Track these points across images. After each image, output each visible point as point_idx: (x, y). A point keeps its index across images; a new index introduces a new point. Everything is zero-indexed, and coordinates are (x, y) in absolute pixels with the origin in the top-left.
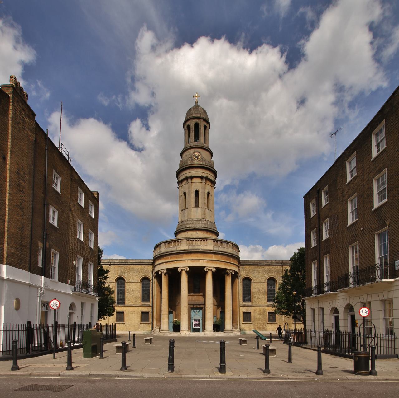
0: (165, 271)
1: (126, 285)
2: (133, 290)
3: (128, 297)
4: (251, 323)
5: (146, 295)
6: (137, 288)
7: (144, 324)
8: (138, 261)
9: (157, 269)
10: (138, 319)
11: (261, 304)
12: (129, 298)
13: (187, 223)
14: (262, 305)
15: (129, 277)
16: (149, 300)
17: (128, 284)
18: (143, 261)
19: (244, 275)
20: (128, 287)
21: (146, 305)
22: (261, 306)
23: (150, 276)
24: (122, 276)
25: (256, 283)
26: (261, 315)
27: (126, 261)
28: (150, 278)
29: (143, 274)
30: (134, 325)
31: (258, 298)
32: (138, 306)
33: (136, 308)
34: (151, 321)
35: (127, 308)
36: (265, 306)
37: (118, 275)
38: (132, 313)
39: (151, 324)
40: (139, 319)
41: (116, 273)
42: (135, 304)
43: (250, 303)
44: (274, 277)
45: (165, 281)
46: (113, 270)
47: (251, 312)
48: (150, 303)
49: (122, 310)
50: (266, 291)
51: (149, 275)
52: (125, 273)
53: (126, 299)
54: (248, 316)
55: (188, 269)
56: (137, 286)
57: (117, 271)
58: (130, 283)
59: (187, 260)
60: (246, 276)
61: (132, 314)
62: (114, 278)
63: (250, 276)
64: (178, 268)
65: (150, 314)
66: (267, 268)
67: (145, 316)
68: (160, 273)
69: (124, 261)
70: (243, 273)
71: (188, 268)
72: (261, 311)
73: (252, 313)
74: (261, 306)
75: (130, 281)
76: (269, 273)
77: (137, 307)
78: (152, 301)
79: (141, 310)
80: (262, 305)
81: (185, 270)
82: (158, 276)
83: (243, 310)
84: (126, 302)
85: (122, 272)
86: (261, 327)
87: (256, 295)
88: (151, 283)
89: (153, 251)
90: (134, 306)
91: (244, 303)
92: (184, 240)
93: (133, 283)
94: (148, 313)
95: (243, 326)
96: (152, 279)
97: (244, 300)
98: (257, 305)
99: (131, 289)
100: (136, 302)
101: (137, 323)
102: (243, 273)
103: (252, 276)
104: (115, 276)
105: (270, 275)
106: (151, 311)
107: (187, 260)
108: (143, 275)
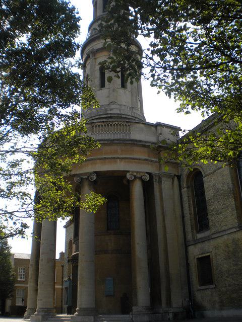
4: (213, 286)
11: (226, 228)
14: (228, 230)
22: (227, 232)
25: (210, 174)
26: (231, 260)
31: (219, 212)
36: (234, 230)
47: (209, 256)
55: (94, 177)
72: (228, 247)
73: (214, 261)
74: (227, 232)
80: (228, 230)
86: (235, 295)
87: (213, 207)
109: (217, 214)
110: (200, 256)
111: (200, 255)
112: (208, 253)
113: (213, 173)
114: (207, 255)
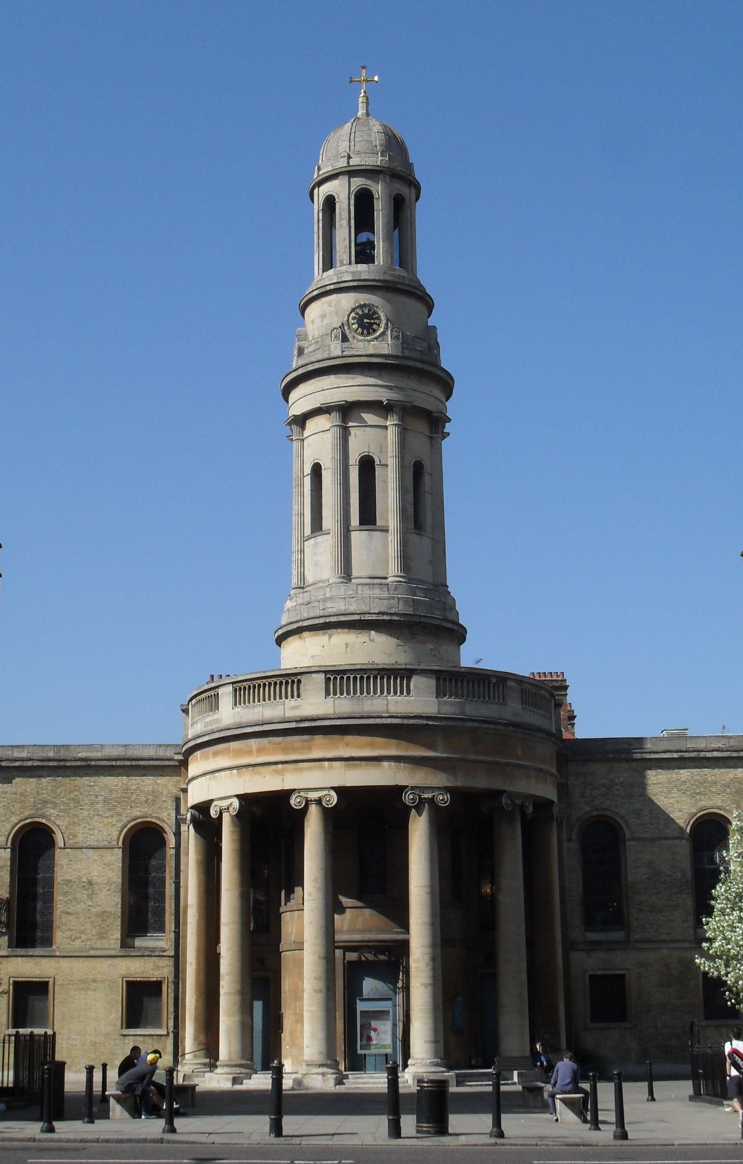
0: (236, 803)
1: (61, 858)
2: (90, 883)
3: (68, 913)
4: (626, 1025)
5: (142, 907)
6: (110, 874)
7: (141, 1038)
8: (115, 753)
9: (196, 794)
10: (112, 1016)
12: (70, 918)
13: (328, 595)
15: (73, 824)
16: (162, 929)
17: (67, 854)
18: (138, 753)
19: (587, 809)
20: (68, 867)
21: (146, 948)
23: (166, 818)
24: (44, 821)
25: (644, 839)
27: (63, 754)
28: (167, 829)
29: (137, 812)
30: (94, 1044)
32: (112, 953)
33: (103, 965)
34: (171, 1024)
35: (65, 964)
36: (687, 945)
37: (27, 813)
38: (86, 984)
39: (171, 1035)
40: (116, 1014)
41: (17, 806)
42: (99, 946)
43: (619, 935)
44: (722, 812)
45: (232, 832)
46: (6, 793)
47: (622, 976)
48: (163, 942)
49: (38, 972)
50: (689, 875)
51: (164, 815)
52: (55, 805)
53: (57, 923)
54: (610, 998)
56: (108, 865)
57: (21, 795)
58: (78, 852)
59: (330, 760)
60: (595, 813)
61: (84, 990)
62: (9, 826)
63: (614, 810)
64: (290, 792)
65: (167, 992)
66: (684, 774)
67: (140, 1002)
68: (213, 813)
69: (51, 754)
70: (583, 796)
71: (333, 793)
74: (670, 945)
75: (80, 839)
76: (698, 794)
77: (110, 961)
78: (177, 934)
79: (123, 972)
81: (319, 802)
82: (206, 822)
83: (590, 963)
84: (60, 937)
85: (45, 802)
88: (173, 852)
89: (183, 711)
90: (92, 953)
91: (592, 936)
92: (314, 675)
93: (91, 852)
94: (158, 984)
95: (589, 1041)
96: (178, 834)
97: (590, 923)
98: (649, 941)
99: (79, 877)
100: (102, 936)
101: (107, 1035)
102: (583, 796)
103: (622, 812)
104: (14, 819)
105: (704, 803)
106: (171, 978)
107: (330, 760)
108: (138, 812)
109: (650, 911)
110: (599, 973)
111: (600, 970)
112: (620, 970)
113: (652, 840)
114: (618, 972)
